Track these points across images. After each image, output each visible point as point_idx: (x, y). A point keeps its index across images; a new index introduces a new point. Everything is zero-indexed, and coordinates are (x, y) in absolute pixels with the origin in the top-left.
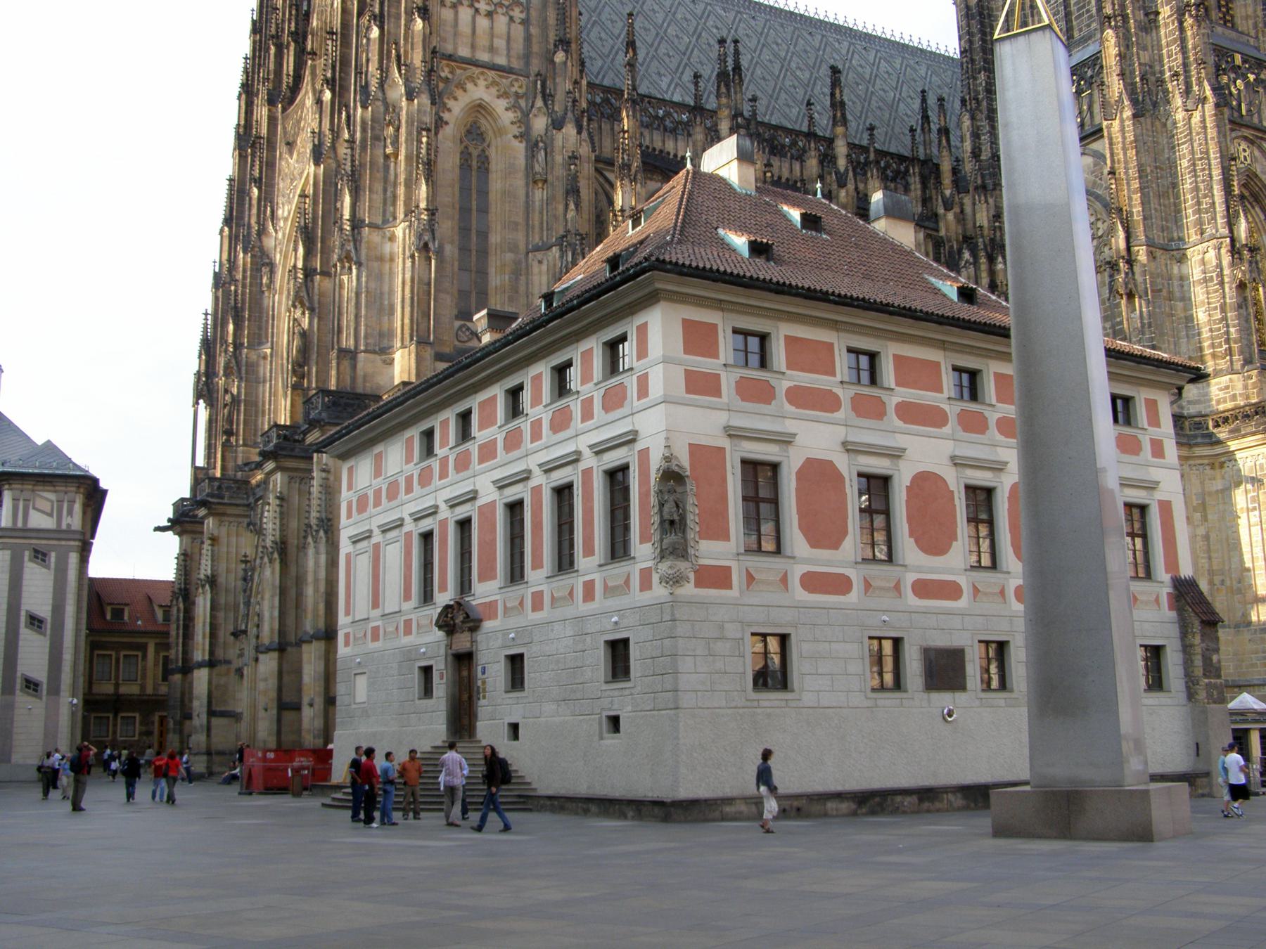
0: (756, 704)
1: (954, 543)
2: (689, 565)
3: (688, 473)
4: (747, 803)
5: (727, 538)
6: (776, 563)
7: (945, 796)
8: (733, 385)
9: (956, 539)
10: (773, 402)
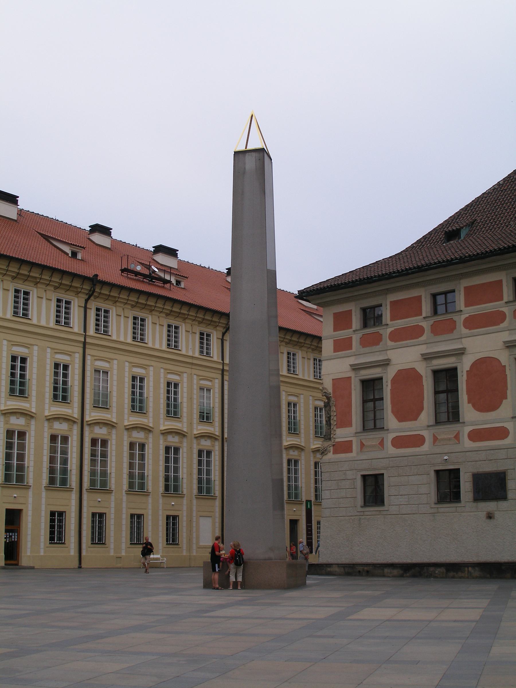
0: (362, 514)
1: (504, 401)
2: (330, 443)
3: (331, 395)
4: (338, 567)
5: (351, 425)
6: (378, 435)
7: (466, 569)
8: (359, 340)
9: (506, 398)
10: (381, 343)
